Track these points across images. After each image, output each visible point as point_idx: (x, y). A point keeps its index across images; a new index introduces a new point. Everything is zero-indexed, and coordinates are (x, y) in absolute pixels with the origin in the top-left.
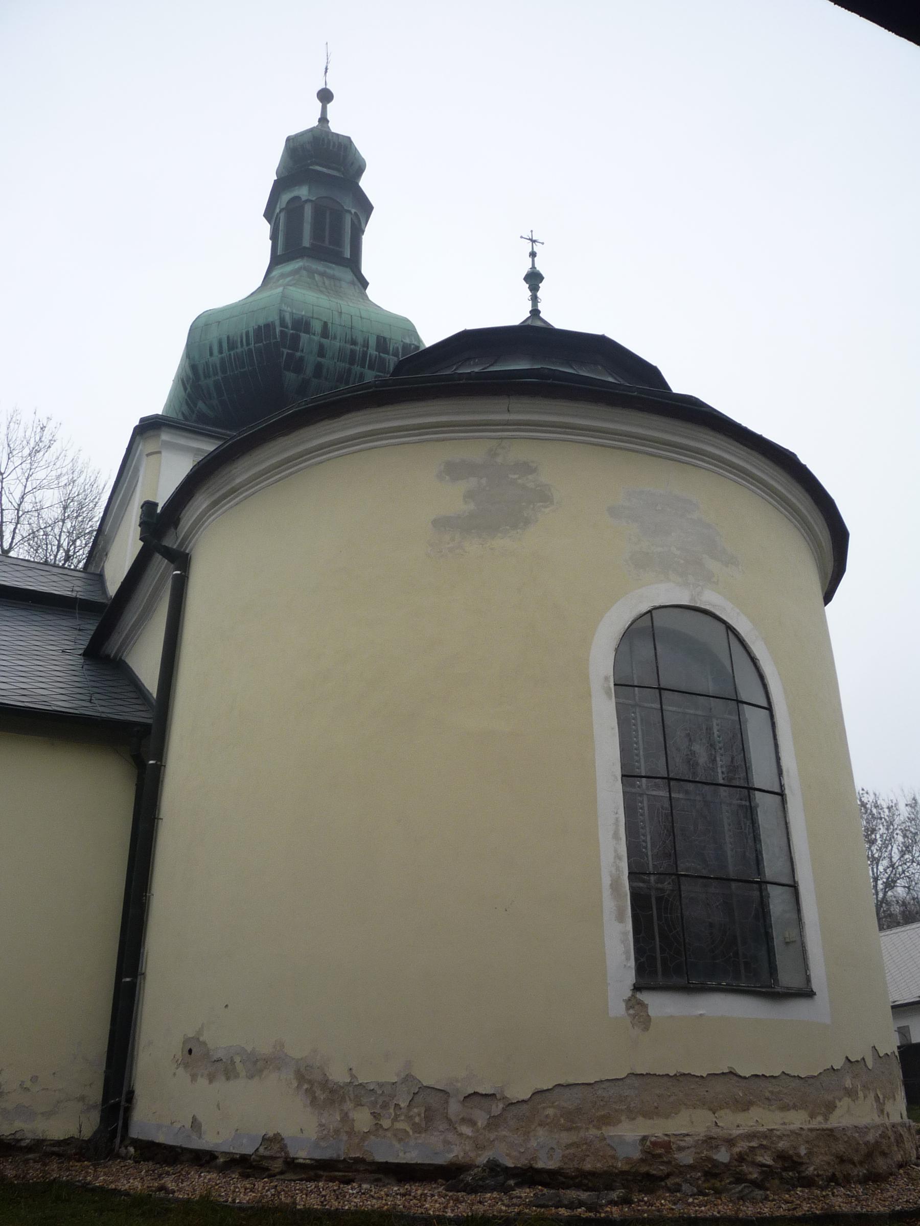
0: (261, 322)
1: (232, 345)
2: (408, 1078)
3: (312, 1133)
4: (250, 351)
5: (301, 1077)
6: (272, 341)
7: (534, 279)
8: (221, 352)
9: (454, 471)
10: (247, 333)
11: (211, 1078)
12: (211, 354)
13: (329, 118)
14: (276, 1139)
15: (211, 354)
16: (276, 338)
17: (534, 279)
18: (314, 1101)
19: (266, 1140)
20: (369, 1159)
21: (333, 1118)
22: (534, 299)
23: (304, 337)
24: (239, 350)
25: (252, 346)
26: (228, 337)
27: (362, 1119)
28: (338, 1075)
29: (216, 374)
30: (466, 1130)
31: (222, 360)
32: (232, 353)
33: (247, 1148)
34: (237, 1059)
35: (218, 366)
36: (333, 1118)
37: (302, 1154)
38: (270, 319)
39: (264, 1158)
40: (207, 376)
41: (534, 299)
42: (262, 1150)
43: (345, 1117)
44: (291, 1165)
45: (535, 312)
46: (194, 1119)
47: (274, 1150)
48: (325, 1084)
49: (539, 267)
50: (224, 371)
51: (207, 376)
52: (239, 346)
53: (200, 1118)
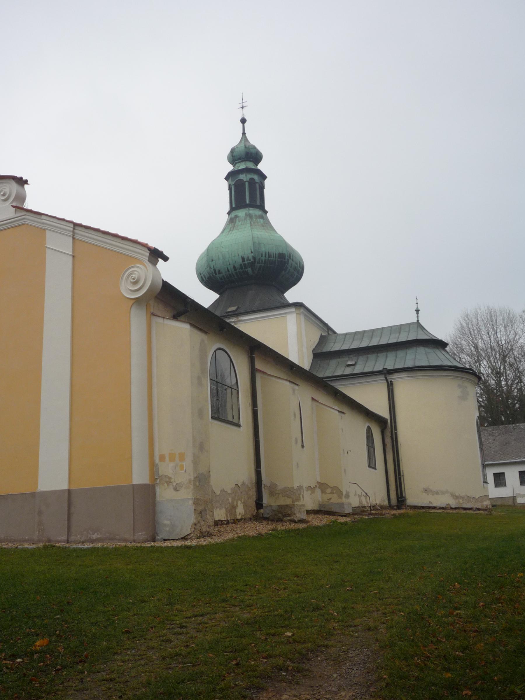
0: (281, 252)
1: (270, 256)
2: (466, 495)
4: (275, 260)
5: (451, 495)
6: (284, 260)
7: (417, 311)
8: (265, 256)
9: (459, 386)
10: (276, 254)
12: (262, 256)
13: (246, 132)
14: (449, 504)
15: (262, 256)
16: (285, 259)
17: (417, 311)
18: (454, 498)
19: (447, 504)
20: (462, 507)
22: (418, 317)
23: (290, 260)
24: (272, 259)
25: (277, 259)
26: (269, 253)
27: (461, 501)
28: (457, 494)
29: (261, 263)
30: (473, 503)
31: (265, 260)
32: (269, 258)
33: (443, 506)
34: (439, 492)
35: (263, 261)
37: (453, 506)
38: (284, 252)
39: (447, 507)
40: (258, 263)
41: (418, 317)
42: (447, 506)
43: (459, 501)
44: (451, 508)
45: (418, 321)
46: (430, 502)
47: (448, 506)
48: (455, 496)
49: (419, 308)
50: (265, 263)
51: (258, 263)
52: (272, 257)
53: (431, 501)
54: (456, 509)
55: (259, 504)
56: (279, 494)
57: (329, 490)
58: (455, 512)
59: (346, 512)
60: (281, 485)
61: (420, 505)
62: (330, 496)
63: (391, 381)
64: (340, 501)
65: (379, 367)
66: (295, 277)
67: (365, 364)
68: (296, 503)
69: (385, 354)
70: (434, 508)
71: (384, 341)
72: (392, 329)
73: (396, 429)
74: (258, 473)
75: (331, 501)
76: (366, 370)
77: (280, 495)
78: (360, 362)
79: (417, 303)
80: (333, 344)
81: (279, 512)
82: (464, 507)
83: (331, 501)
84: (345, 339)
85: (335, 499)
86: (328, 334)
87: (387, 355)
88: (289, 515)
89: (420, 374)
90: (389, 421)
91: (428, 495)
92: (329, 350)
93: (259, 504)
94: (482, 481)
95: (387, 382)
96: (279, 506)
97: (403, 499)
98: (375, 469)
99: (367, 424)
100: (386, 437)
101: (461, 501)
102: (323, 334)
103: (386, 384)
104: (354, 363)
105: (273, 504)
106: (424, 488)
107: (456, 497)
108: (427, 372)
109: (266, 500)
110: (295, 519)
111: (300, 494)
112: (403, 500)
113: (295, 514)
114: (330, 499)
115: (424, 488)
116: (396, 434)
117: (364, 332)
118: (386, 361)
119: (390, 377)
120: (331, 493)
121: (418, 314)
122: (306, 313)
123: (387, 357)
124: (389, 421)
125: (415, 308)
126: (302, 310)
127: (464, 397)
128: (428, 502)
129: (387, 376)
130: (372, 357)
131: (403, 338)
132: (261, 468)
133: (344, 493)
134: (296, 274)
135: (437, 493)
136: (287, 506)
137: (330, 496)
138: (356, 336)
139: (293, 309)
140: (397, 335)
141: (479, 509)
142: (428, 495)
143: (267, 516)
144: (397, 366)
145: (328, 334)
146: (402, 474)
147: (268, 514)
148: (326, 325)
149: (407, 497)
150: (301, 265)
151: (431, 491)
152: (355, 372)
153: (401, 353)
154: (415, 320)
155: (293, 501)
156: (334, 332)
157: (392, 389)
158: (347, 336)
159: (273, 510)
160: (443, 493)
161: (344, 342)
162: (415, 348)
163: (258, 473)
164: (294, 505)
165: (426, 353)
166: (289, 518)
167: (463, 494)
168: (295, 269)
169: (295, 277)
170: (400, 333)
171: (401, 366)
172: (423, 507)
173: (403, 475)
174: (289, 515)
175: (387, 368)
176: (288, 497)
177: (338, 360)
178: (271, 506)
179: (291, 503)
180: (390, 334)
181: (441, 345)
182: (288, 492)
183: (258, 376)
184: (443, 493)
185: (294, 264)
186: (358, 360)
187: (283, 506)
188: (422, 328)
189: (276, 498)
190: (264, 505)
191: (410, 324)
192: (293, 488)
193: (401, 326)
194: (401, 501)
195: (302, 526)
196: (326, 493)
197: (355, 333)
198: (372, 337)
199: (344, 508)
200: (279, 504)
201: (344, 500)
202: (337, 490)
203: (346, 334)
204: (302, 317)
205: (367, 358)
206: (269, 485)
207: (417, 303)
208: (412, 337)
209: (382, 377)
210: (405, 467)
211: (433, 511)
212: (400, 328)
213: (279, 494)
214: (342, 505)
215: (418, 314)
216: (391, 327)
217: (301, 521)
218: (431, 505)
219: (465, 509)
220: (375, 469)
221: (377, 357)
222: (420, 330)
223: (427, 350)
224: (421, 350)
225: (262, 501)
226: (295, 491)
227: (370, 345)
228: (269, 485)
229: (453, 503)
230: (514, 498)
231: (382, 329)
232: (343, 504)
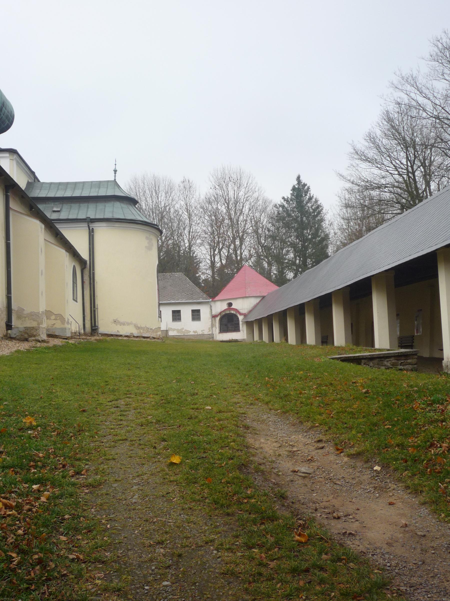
3: (136, 333)
5: (135, 326)
7: (115, 171)
9: (147, 238)
11: (120, 325)
17: (115, 171)
21: (139, 331)
22: (115, 176)
27: (142, 331)
28: (139, 326)
36: (139, 331)
37: (135, 335)
41: (115, 176)
44: (134, 337)
45: (115, 179)
46: (118, 331)
48: (138, 327)
49: (117, 169)
54: (137, 337)
55: (9, 326)
56: (25, 317)
57: (53, 317)
58: (137, 339)
59: (68, 336)
60: (28, 310)
61: (110, 333)
62: (54, 322)
63: (93, 229)
64: (62, 326)
65: (82, 216)
66: (6, 124)
67: (70, 212)
68: (41, 326)
69: (86, 204)
70: (121, 336)
71: (86, 193)
72: (92, 184)
73: (93, 270)
74: (9, 299)
75: (55, 326)
76: (71, 217)
77: (27, 319)
78: (64, 210)
79: (116, 165)
80: (39, 191)
81: (26, 333)
82: (144, 336)
83: (55, 326)
84: (50, 187)
85: (58, 325)
86: (35, 181)
87: (88, 206)
88: (34, 336)
89: (117, 225)
90: (88, 262)
91: (117, 325)
92: (36, 196)
93: (9, 326)
94: (158, 316)
95: (89, 229)
96: (25, 327)
97: (96, 328)
98: (77, 302)
99: (73, 264)
100: (84, 275)
101: (142, 331)
102: (30, 181)
103: (88, 230)
104: (59, 210)
105: (20, 326)
106: (114, 320)
107: (138, 328)
108: (122, 224)
109: (14, 322)
110: (39, 339)
111: (43, 319)
112: (96, 329)
113: (39, 335)
114: (55, 324)
115: (114, 320)
116: (94, 274)
117: (67, 184)
118: (87, 211)
119: (92, 225)
120: (55, 319)
121: (115, 173)
122: (18, 159)
123: (88, 208)
124: (88, 262)
125: (114, 168)
126: (15, 156)
127: (149, 248)
128: (116, 331)
129: (90, 223)
130: (75, 206)
131: (102, 192)
132: (11, 294)
133: (66, 320)
134: (7, 122)
135: (123, 324)
136: (33, 328)
137: (54, 322)
138: (60, 187)
139: (7, 155)
140: (97, 189)
141: (154, 338)
142: (117, 325)
143: (13, 336)
144: (98, 217)
145: (35, 181)
146: (96, 307)
147: (15, 334)
148: (33, 173)
149: (99, 326)
150: (12, 115)
151: (119, 322)
152: (61, 217)
153: (100, 206)
154: (113, 179)
155: (39, 324)
156: (39, 181)
157: (93, 236)
158: (52, 185)
159: (20, 331)
160: (128, 324)
161: (49, 190)
162: (113, 203)
163: (9, 299)
164: (39, 327)
165: (122, 208)
166: (34, 338)
167: (143, 326)
168: (7, 117)
169: (6, 124)
170: (99, 188)
171: (102, 217)
172: (112, 335)
173: (97, 308)
174: (34, 336)
175: (89, 217)
176: (34, 321)
177: (44, 205)
178: (18, 328)
179: (37, 325)
180: (91, 188)
181: (132, 201)
182: (34, 316)
183: (11, 213)
184: (128, 324)
185: (6, 112)
186: (62, 207)
187: (30, 328)
188: (119, 186)
189: (23, 321)
190: (13, 326)
191: (108, 182)
192: (39, 313)
193: (100, 182)
194: (94, 329)
195: (45, 345)
196: (50, 319)
197: (60, 184)
198: (74, 189)
199: (66, 332)
200: (25, 326)
201: (66, 326)
202: (60, 317)
203: (51, 184)
204: (15, 163)
205: (71, 206)
206: (16, 310)
207: (116, 165)
208: (110, 193)
209: (85, 225)
210: (99, 302)
211: (120, 338)
212: (99, 184)
213: (25, 317)
214: (64, 329)
215: (115, 173)
216: (92, 182)
217: (43, 341)
218: (118, 334)
219: (144, 337)
220: (77, 302)
221: (80, 207)
222: (116, 187)
223: (123, 205)
224: (118, 205)
225: (11, 323)
226: (40, 316)
227: (74, 195)
228: (16, 310)
229: (136, 332)
230: (167, 331)
231: (84, 183)
232: (65, 329)
